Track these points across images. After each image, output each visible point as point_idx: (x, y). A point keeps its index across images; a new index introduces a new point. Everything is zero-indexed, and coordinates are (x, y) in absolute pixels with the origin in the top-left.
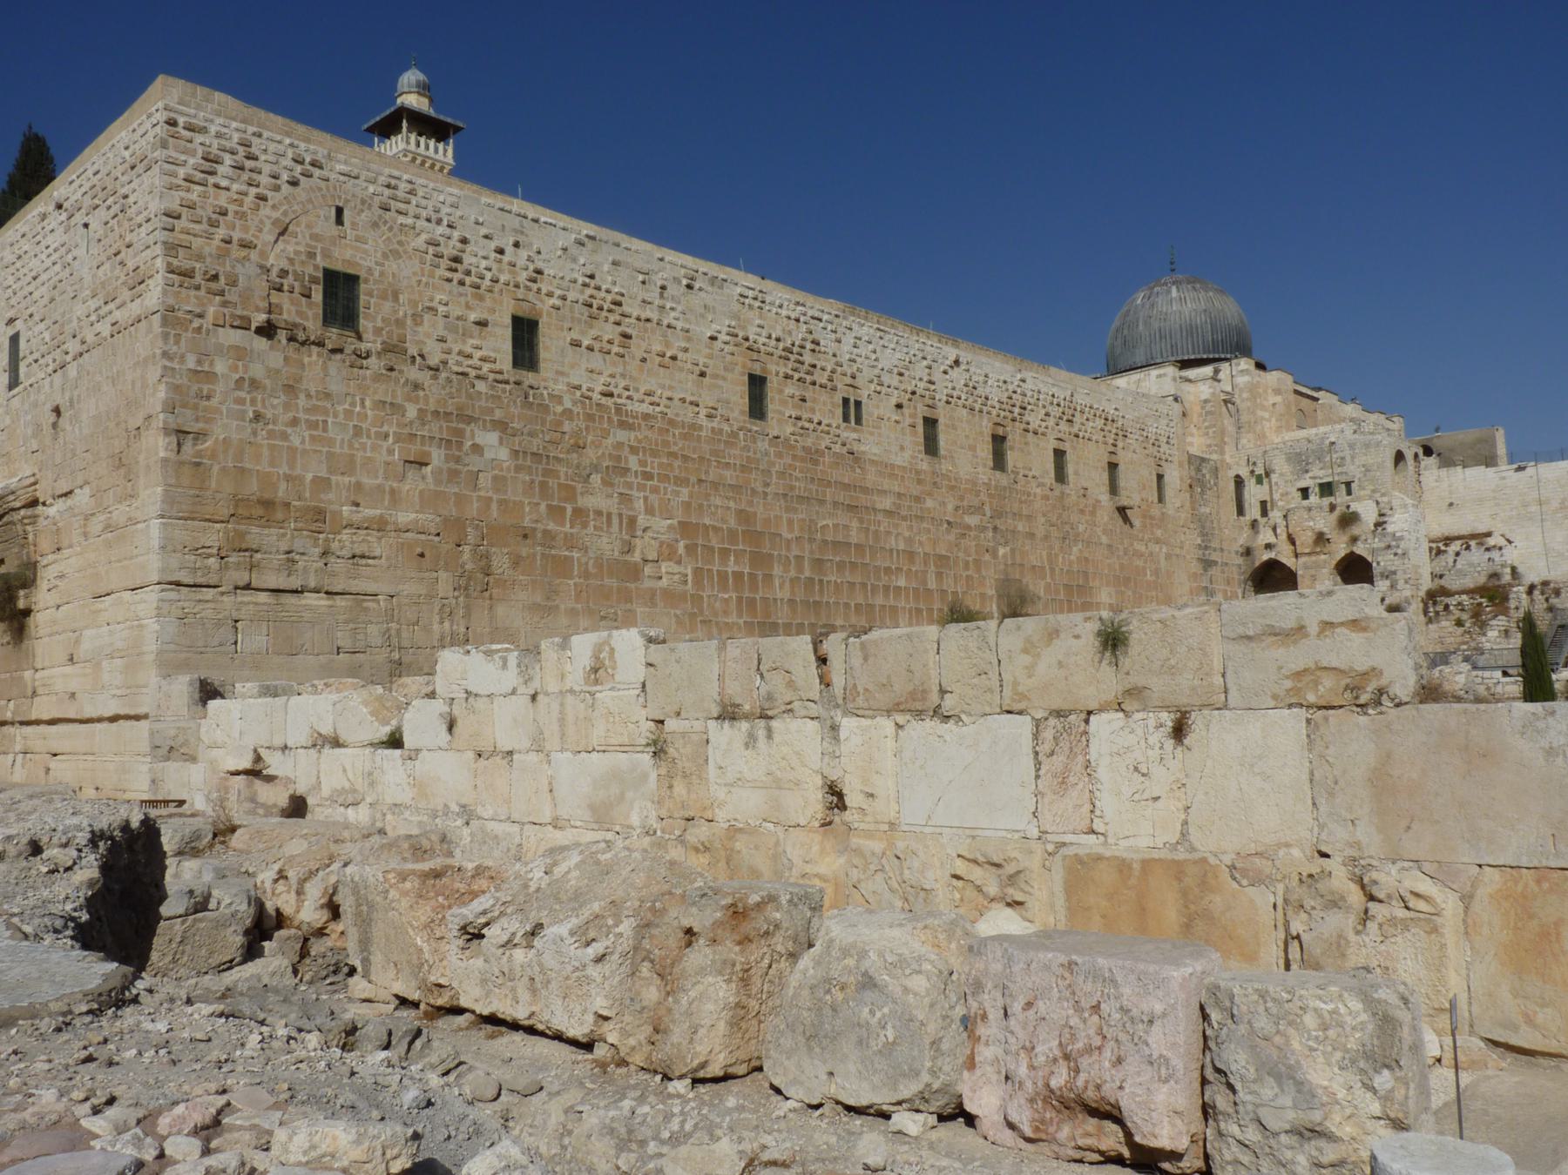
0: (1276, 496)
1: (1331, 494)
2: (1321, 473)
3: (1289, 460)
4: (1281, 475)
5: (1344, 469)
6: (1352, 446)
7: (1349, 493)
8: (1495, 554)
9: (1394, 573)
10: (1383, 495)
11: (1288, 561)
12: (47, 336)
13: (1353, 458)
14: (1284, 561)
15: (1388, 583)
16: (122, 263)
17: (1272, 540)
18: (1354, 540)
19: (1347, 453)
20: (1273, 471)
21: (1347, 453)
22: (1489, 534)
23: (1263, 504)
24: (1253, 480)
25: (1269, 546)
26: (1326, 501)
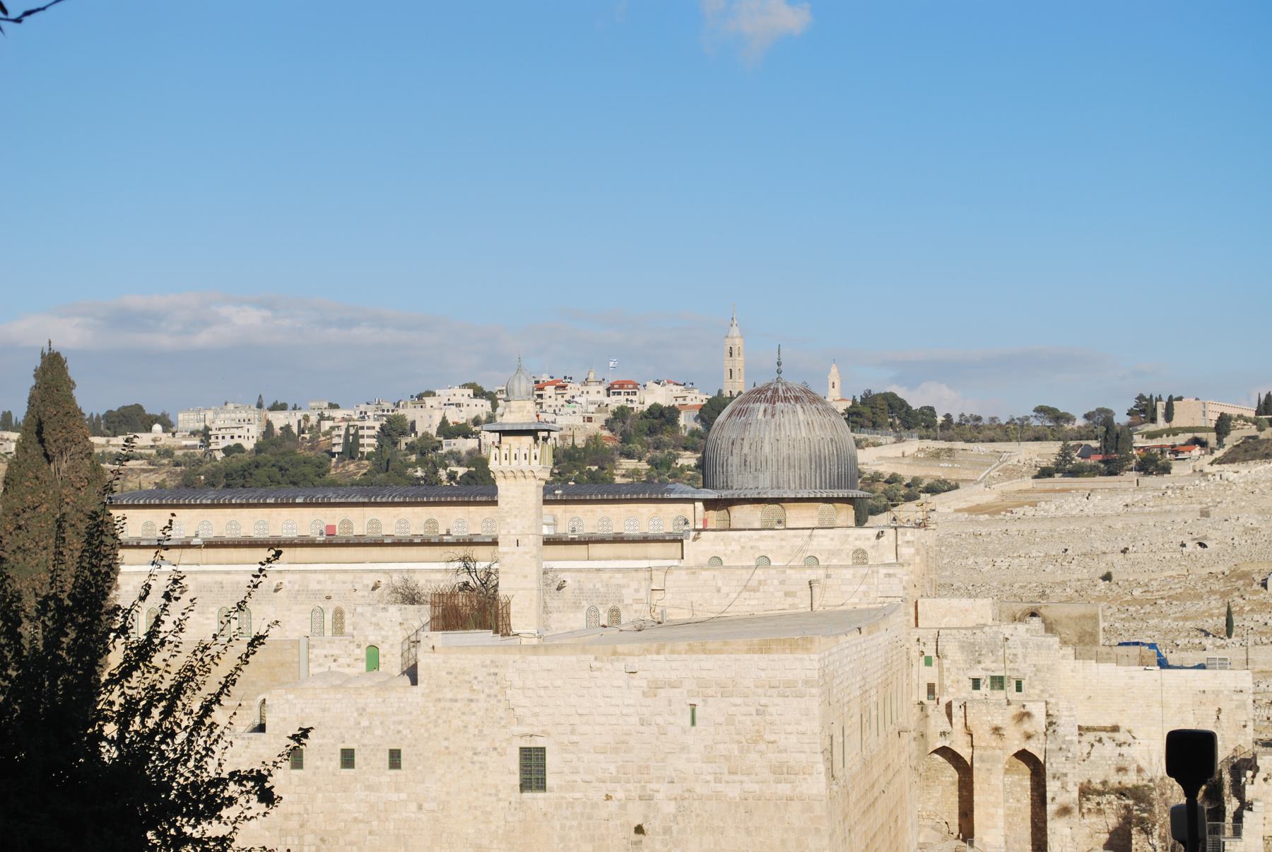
0: (947, 682)
1: (1002, 688)
2: (993, 666)
3: (962, 647)
4: (954, 661)
5: (1016, 666)
6: (1025, 645)
7: (1019, 689)
8: (1124, 749)
9: (1065, 775)
10: (1051, 696)
11: (965, 753)
12: (613, 769)
13: (1025, 656)
14: (958, 751)
15: (1058, 784)
16: (761, 753)
17: (947, 727)
18: (1029, 737)
19: (1020, 651)
20: (945, 657)
21: (1020, 651)
22: (1115, 729)
23: (931, 689)
24: (922, 660)
25: (943, 734)
26: (999, 695)
